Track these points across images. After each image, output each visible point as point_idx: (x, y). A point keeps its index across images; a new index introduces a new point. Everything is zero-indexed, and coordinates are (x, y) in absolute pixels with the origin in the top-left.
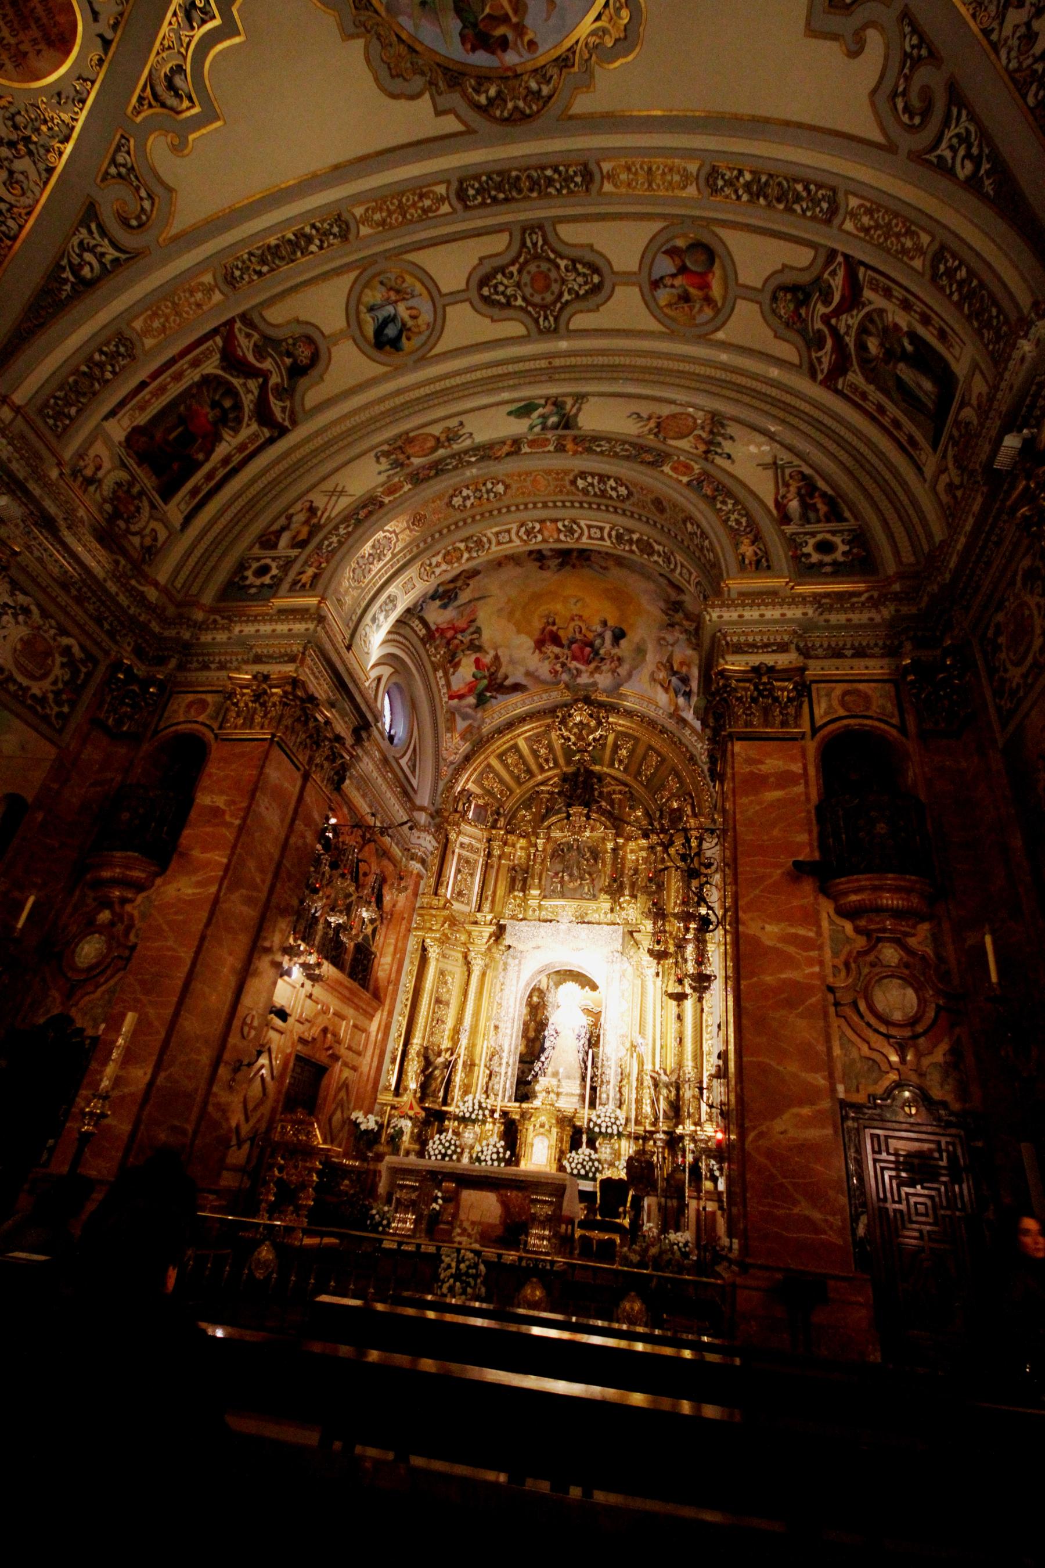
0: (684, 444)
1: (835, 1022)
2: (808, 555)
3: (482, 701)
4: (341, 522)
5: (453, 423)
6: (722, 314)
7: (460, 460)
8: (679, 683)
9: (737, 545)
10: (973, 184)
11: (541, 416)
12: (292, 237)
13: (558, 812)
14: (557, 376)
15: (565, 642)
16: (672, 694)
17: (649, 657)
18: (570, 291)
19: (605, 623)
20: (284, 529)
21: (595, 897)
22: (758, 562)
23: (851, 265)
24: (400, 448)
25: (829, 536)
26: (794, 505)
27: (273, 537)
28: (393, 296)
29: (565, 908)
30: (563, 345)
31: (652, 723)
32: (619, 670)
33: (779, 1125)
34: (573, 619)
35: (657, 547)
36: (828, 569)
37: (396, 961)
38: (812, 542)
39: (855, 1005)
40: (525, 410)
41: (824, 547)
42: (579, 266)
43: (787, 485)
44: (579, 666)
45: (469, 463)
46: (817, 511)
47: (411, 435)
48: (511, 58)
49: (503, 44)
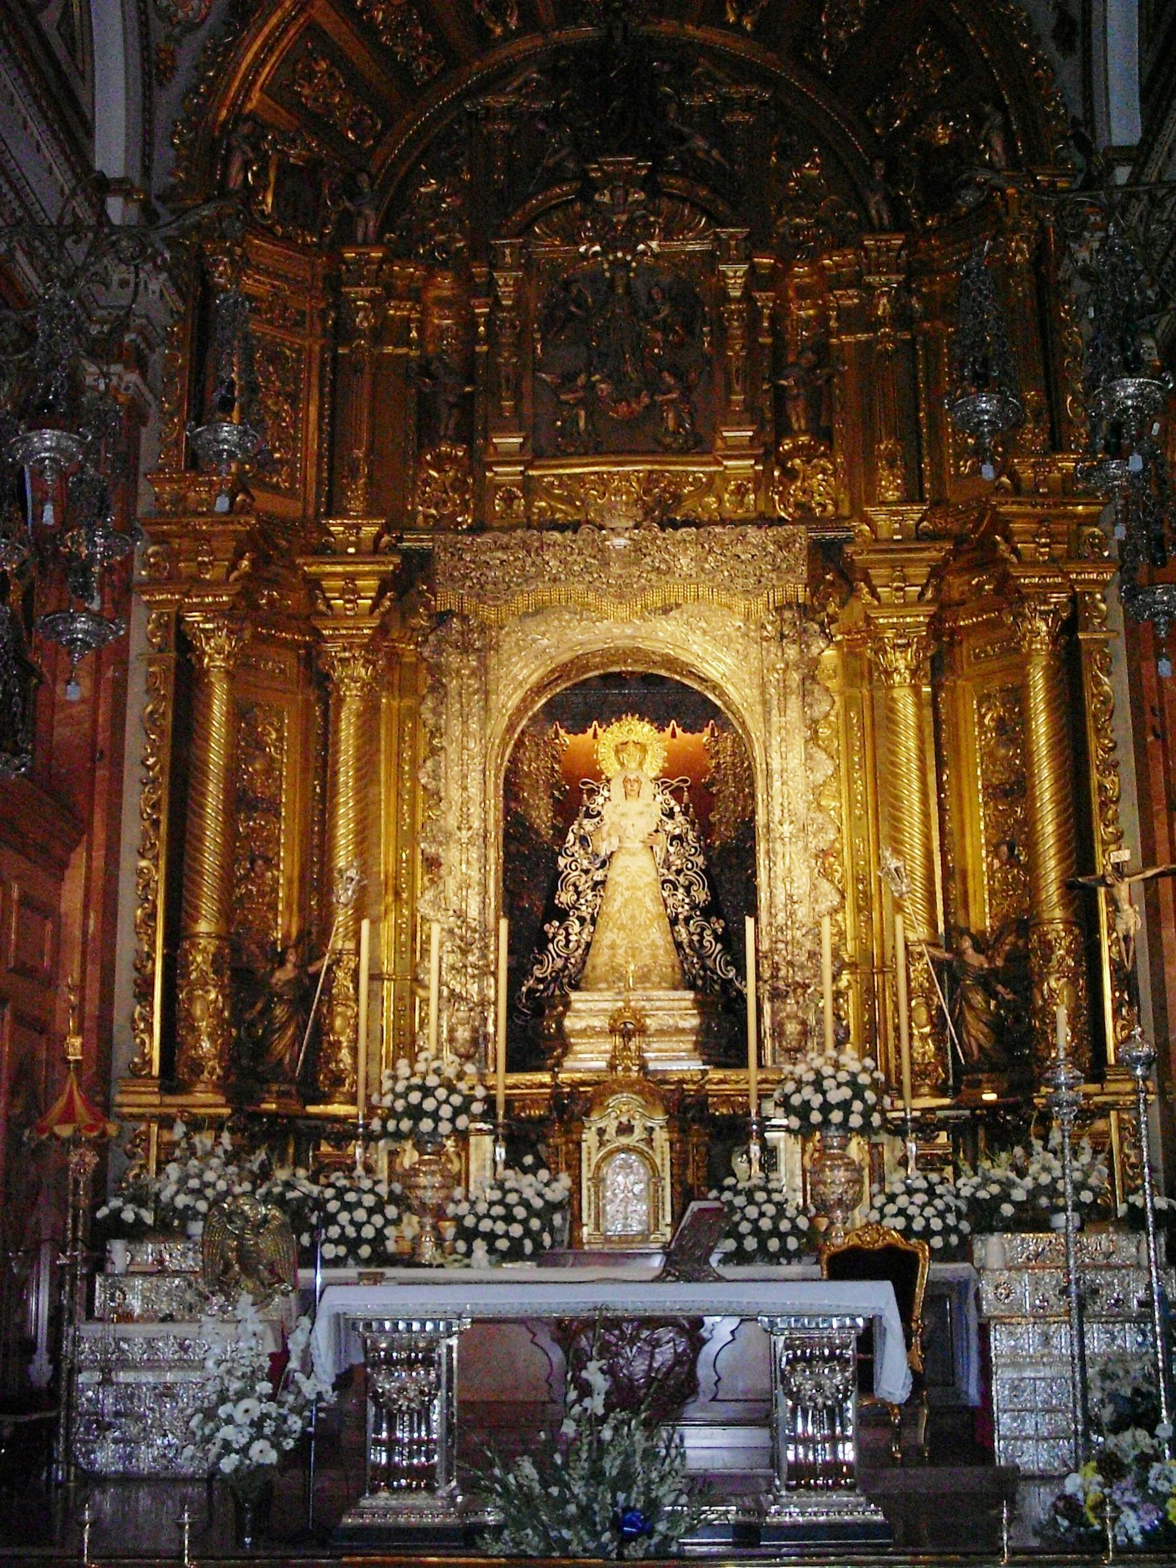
13: (556, 176)
37: (105, 696)
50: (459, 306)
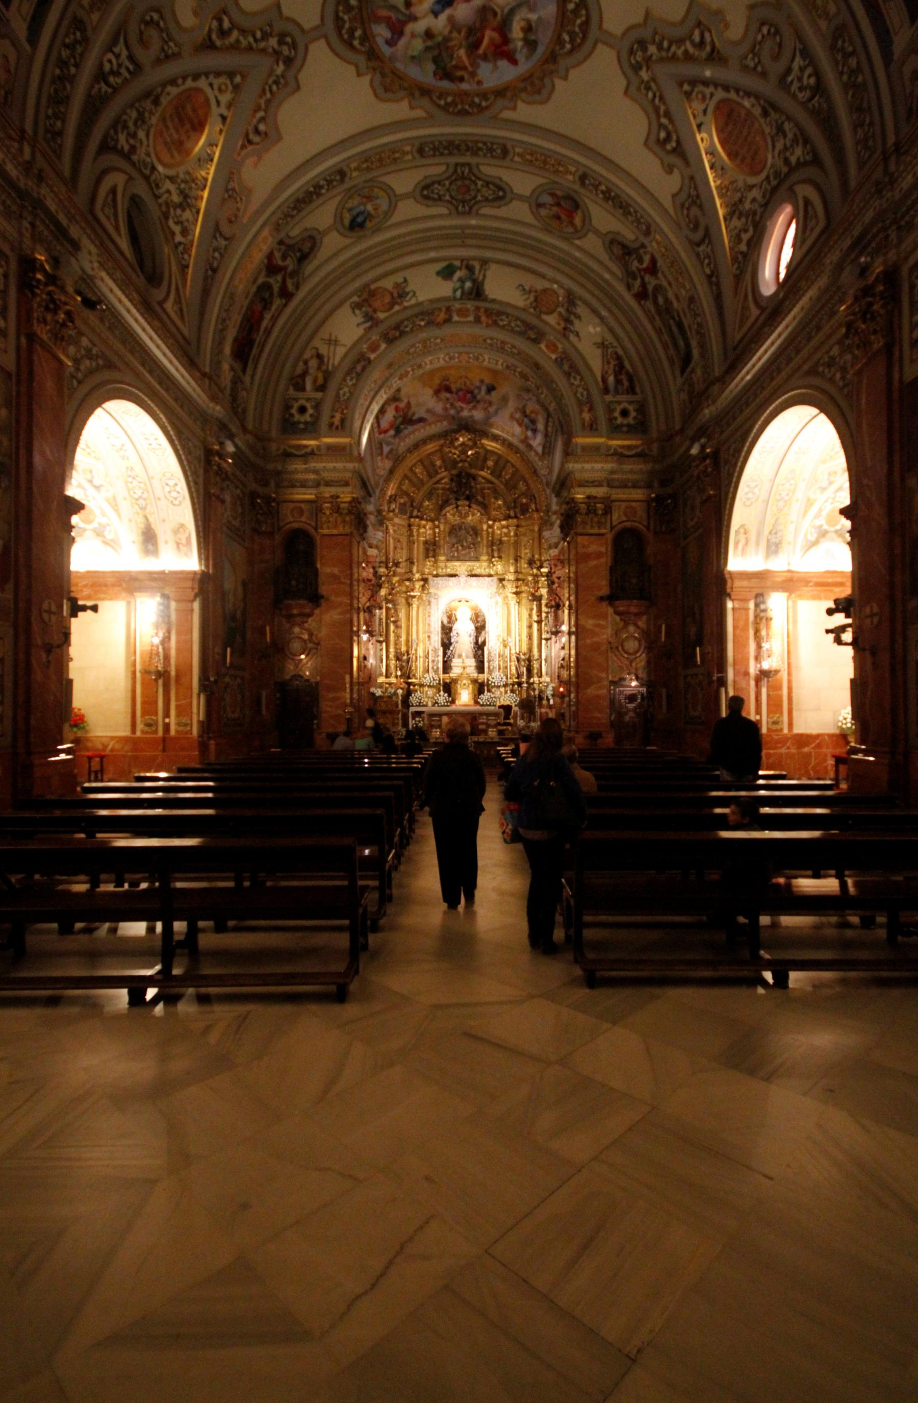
0: (552, 319)
1: (610, 654)
2: (616, 418)
3: (398, 431)
5: (399, 278)
6: (580, 233)
7: (414, 323)
9: (581, 412)
10: (709, 277)
12: (312, 189)
15: (454, 390)
16: (524, 428)
18: (482, 196)
19: (482, 381)
20: (305, 374)
22: (591, 425)
23: (653, 261)
24: (366, 300)
26: (611, 379)
27: (300, 380)
28: (365, 200)
29: (461, 567)
30: (473, 222)
31: (510, 446)
33: (589, 691)
36: (625, 429)
39: (617, 648)
40: (447, 273)
41: (625, 413)
42: (491, 186)
43: (609, 363)
45: (420, 326)
46: (623, 385)
47: (373, 287)
48: (465, 86)
49: (461, 79)
50: (433, 529)
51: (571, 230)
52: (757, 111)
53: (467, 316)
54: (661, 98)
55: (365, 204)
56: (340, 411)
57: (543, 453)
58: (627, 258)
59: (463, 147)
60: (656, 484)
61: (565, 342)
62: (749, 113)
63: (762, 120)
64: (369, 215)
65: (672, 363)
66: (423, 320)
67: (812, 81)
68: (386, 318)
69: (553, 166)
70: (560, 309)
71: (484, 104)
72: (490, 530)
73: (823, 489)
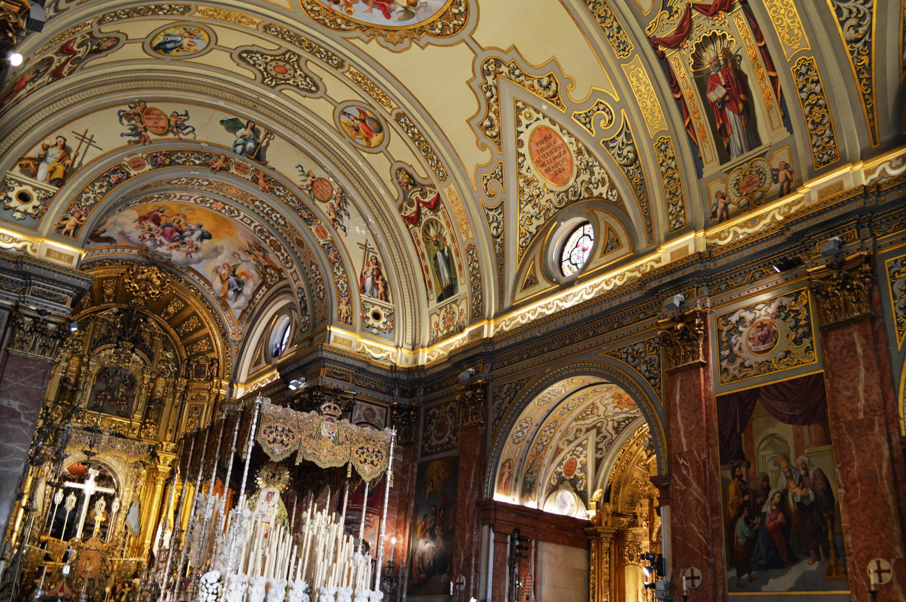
0: (324, 207)
4: (97, 180)
5: (181, 109)
8: (235, 283)
9: (339, 302)
11: (243, 137)
12: (153, 7)
14: (259, 108)
15: (162, 223)
17: (220, 258)
20: (41, 159)
21: (127, 415)
22: (347, 318)
23: (438, 200)
24: (139, 115)
25: (379, 309)
26: (369, 281)
32: (193, 255)
34: (178, 215)
35: (283, 251)
38: (372, 310)
40: (232, 125)
43: (369, 266)
44: (163, 240)
45: (195, 164)
47: (149, 105)
51: (364, 143)
52: (573, 148)
53: (246, 173)
54: (497, 100)
55: (183, 37)
56: (77, 215)
57: (240, 318)
58: (410, 187)
59: (306, 44)
60: (397, 392)
61: (334, 231)
62: (564, 144)
63: (574, 155)
64: (181, 46)
65: (428, 284)
66: (199, 159)
67: (631, 156)
68: (157, 140)
69: (378, 95)
70: (332, 201)
71: (343, 26)
72: (152, 385)
73: (570, 442)
